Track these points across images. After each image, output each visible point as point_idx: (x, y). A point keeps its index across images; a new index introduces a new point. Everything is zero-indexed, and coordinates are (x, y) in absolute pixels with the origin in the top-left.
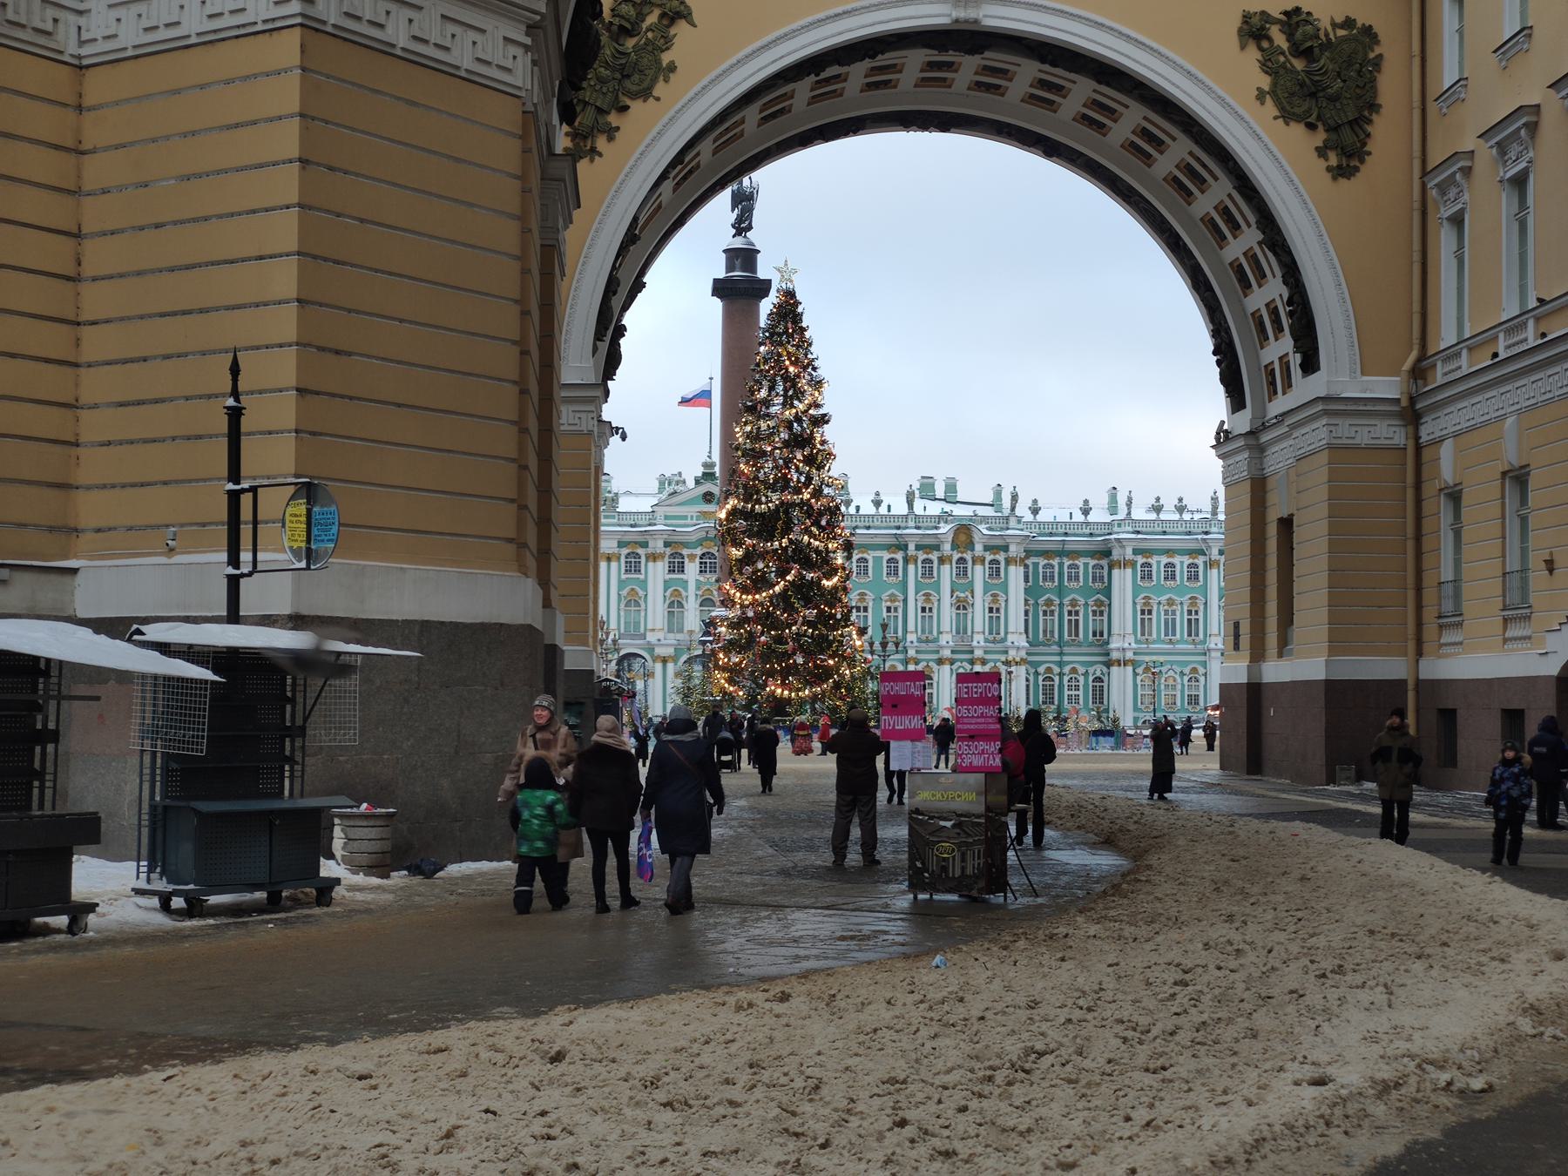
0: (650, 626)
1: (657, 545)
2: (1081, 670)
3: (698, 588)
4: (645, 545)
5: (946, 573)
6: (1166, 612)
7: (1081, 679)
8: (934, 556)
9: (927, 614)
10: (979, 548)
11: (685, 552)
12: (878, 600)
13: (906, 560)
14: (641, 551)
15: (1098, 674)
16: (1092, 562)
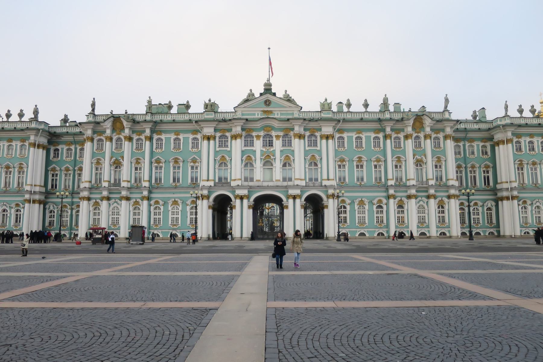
0: (233, 178)
1: (237, 129)
2: (480, 204)
3: (262, 155)
4: (230, 130)
5: (409, 144)
6: (532, 169)
7: (480, 209)
8: (401, 135)
9: (398, 169)
10: (428, 130)
11: (254, 134)
12: (369, 161)
13: (386, 137)
14: (228, 134)
15: (489, 206)
16: (481, 144)
